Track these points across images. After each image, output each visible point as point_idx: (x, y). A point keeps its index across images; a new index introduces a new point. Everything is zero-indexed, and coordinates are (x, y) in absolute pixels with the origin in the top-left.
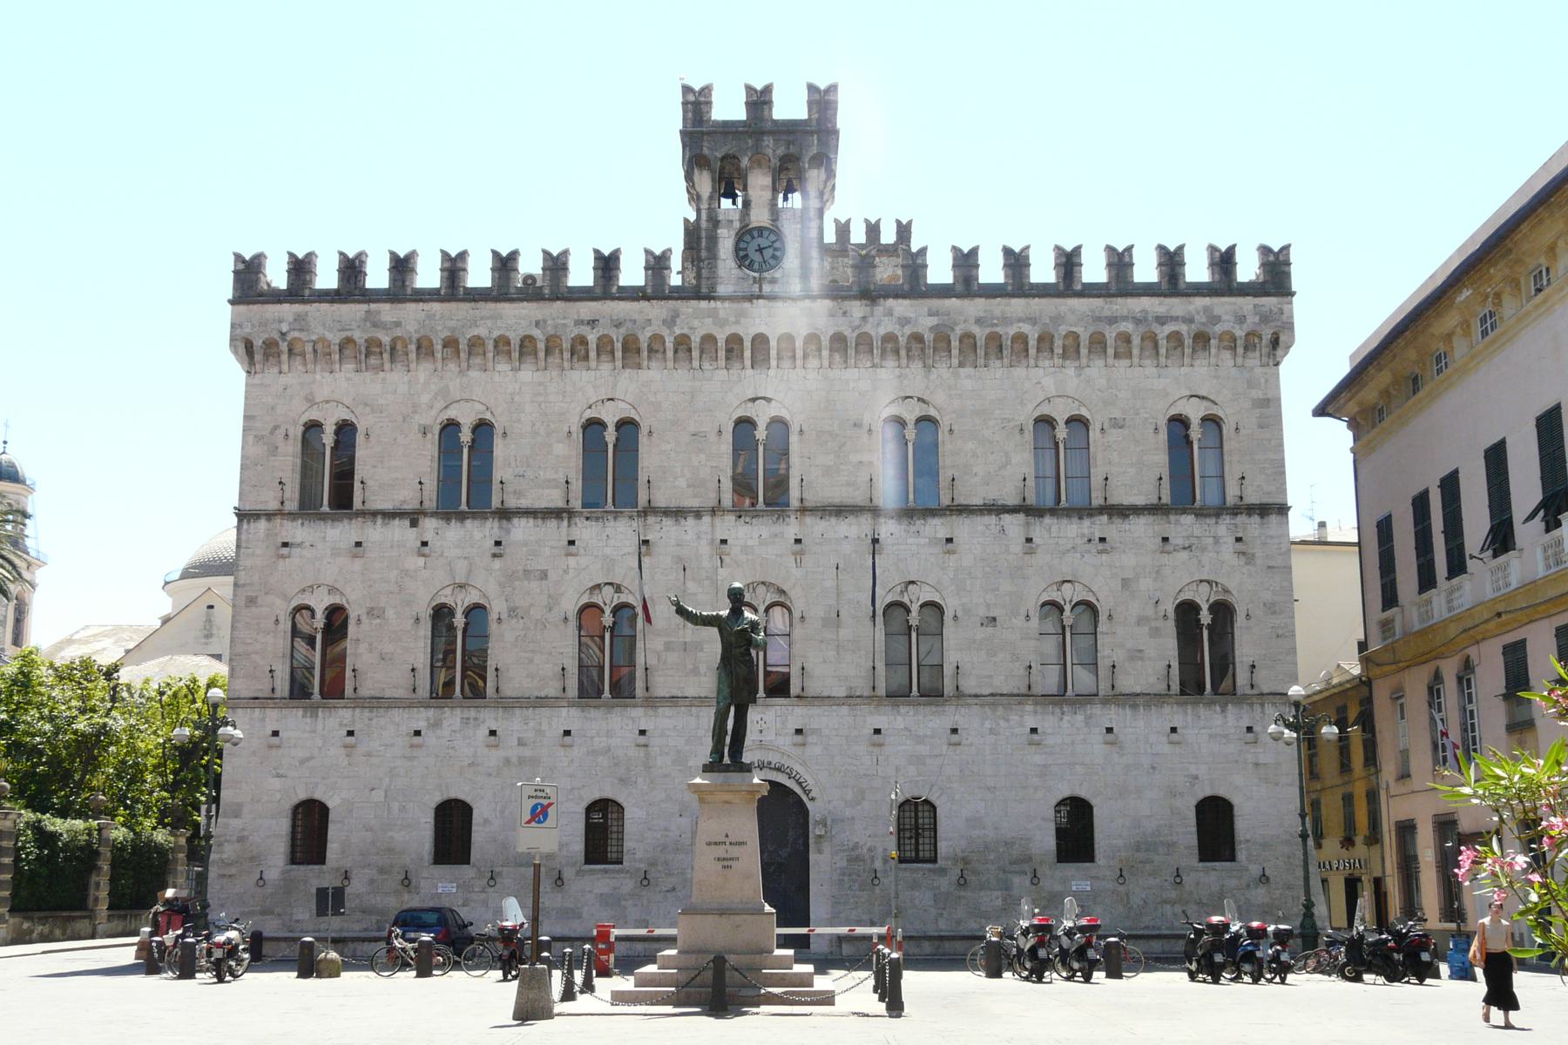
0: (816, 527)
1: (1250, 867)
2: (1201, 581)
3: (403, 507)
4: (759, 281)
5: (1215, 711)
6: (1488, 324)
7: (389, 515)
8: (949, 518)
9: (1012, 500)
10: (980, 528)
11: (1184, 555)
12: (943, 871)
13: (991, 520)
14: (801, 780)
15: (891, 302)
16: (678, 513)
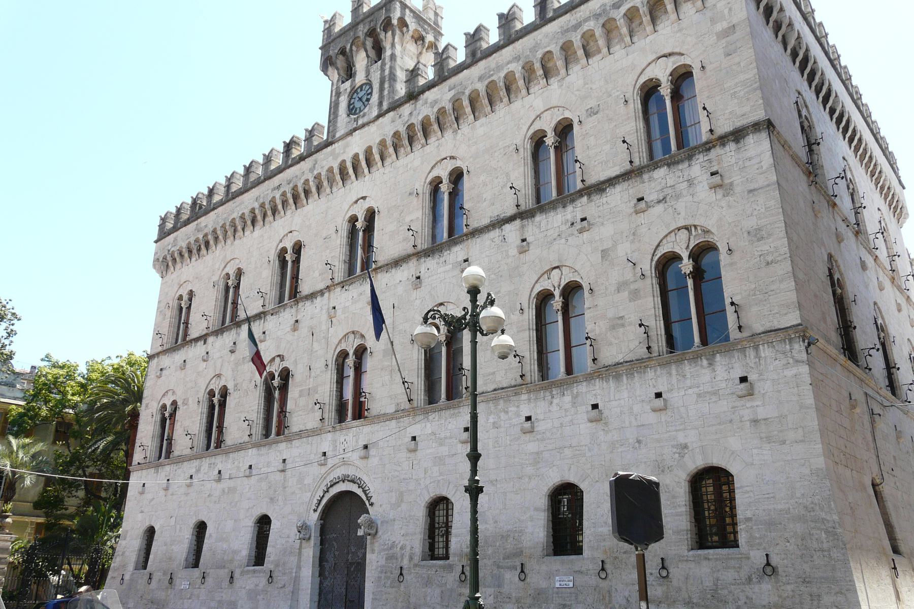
1: (752, 553)
2: (679, 229)
4: (356, 120)
5: (702, 366)
8: (466, 243)
9: (511, 211)
10: (488, 242)
11: (659, 208)
12: (450, 568)
13: (495, 234)
14: (367, 488)
15: (427, 94)
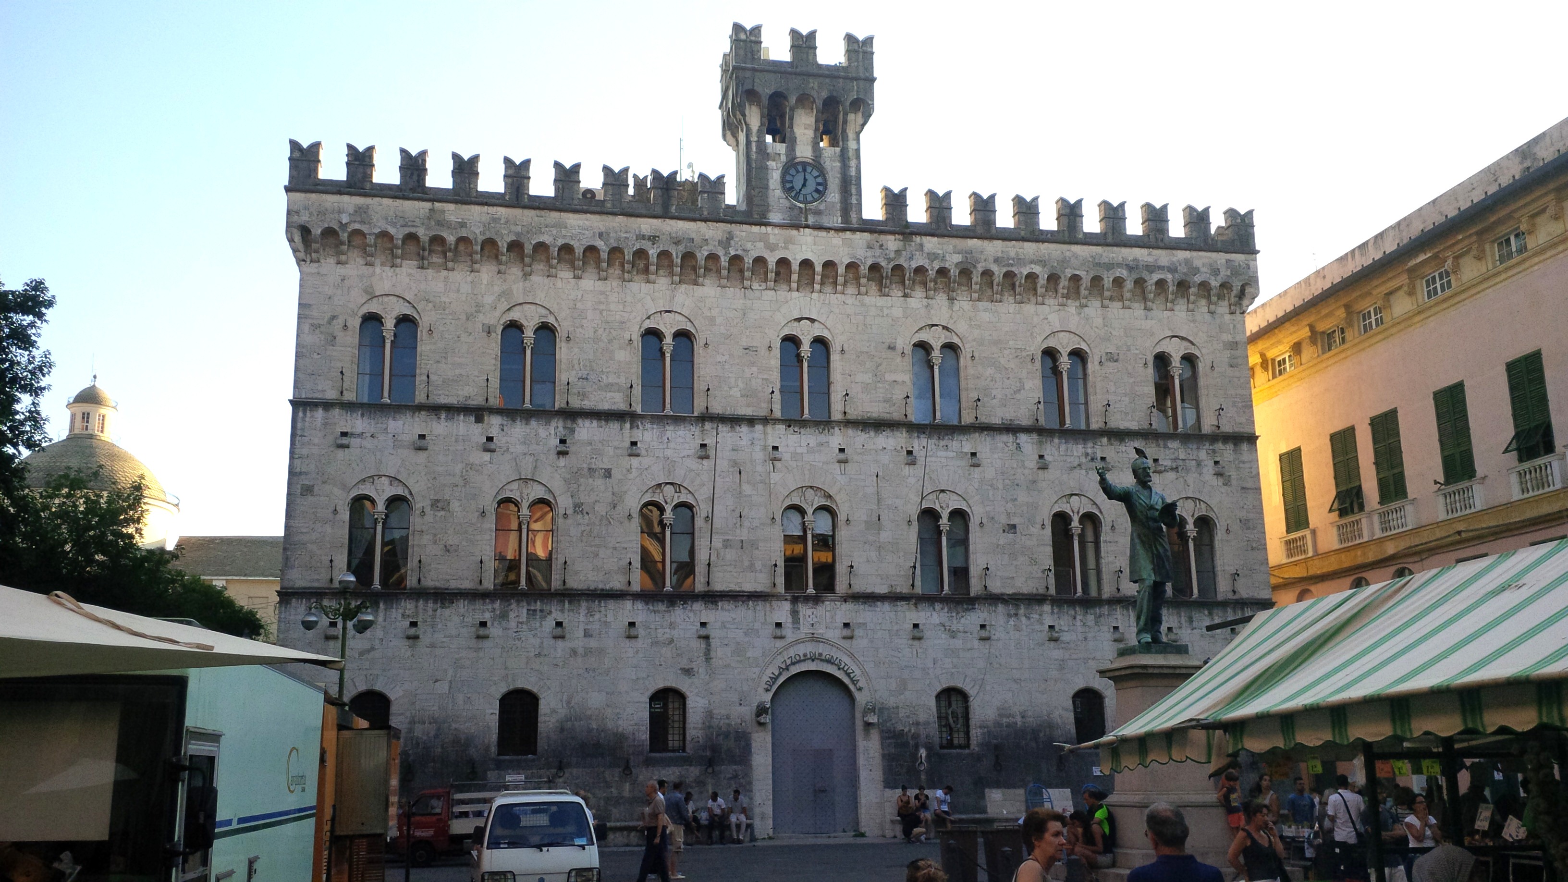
0: (858, 439)
2: (1187, 498)
3: (467, 403)
6: (1438, 285)
7: (452, 410)
9: (1026, 422)
10: (1000, 445)
11: (1171, 475)
13: (1009, 438)
16: (734, 421)
